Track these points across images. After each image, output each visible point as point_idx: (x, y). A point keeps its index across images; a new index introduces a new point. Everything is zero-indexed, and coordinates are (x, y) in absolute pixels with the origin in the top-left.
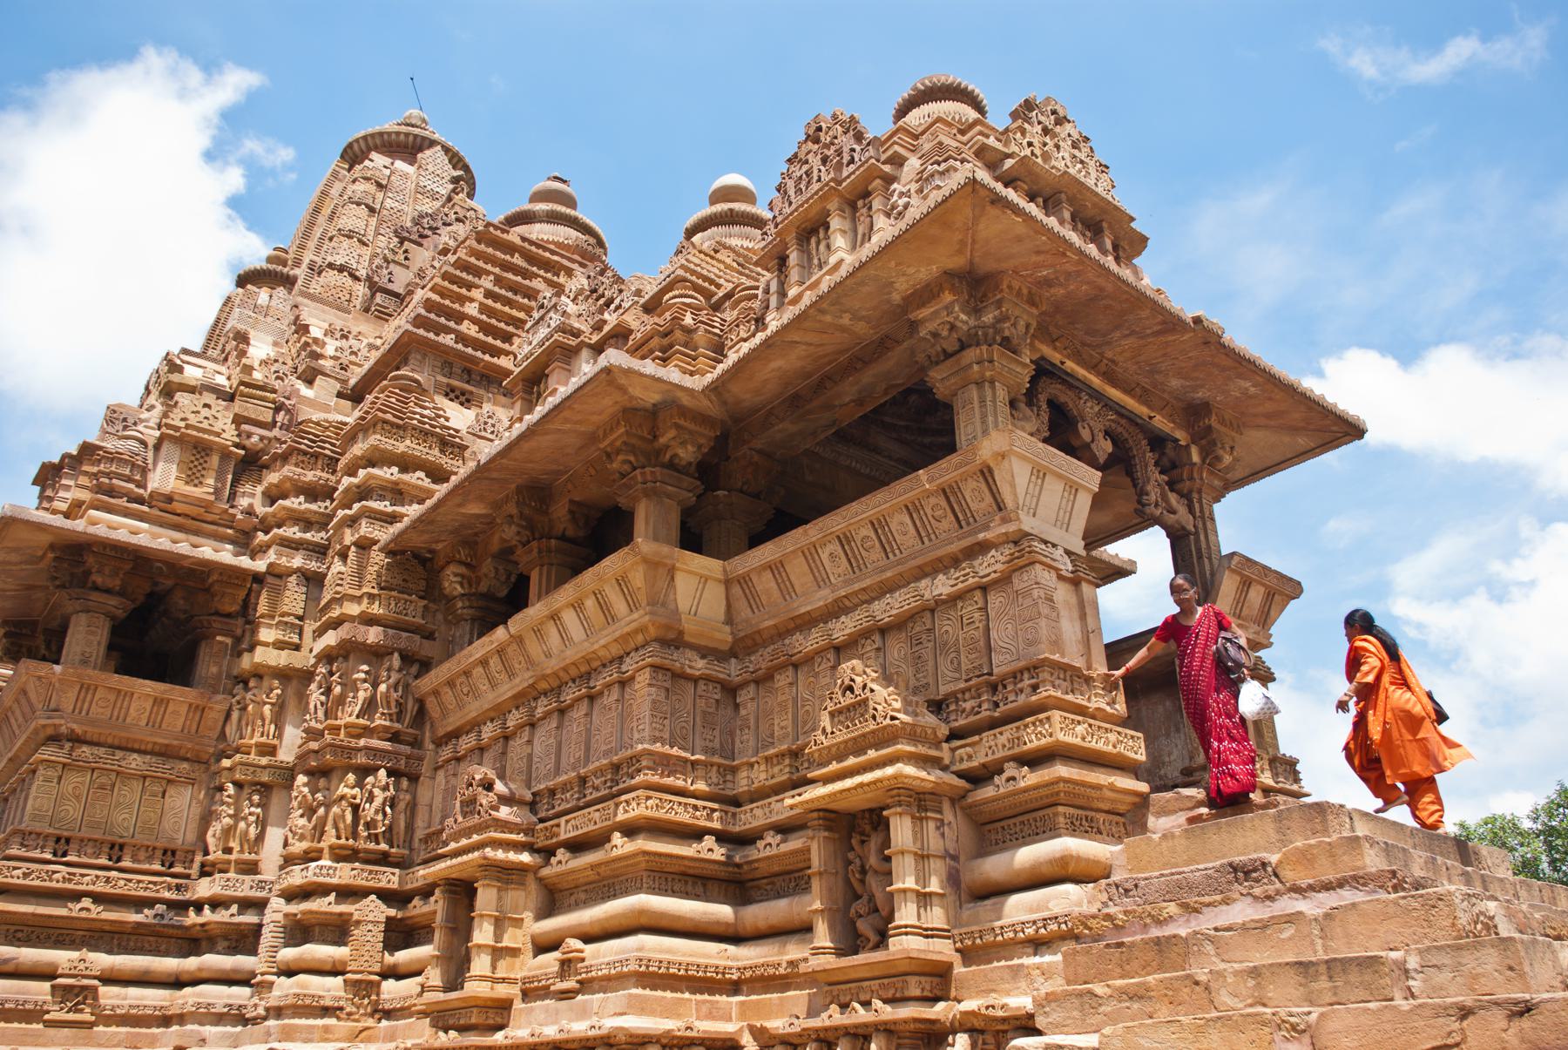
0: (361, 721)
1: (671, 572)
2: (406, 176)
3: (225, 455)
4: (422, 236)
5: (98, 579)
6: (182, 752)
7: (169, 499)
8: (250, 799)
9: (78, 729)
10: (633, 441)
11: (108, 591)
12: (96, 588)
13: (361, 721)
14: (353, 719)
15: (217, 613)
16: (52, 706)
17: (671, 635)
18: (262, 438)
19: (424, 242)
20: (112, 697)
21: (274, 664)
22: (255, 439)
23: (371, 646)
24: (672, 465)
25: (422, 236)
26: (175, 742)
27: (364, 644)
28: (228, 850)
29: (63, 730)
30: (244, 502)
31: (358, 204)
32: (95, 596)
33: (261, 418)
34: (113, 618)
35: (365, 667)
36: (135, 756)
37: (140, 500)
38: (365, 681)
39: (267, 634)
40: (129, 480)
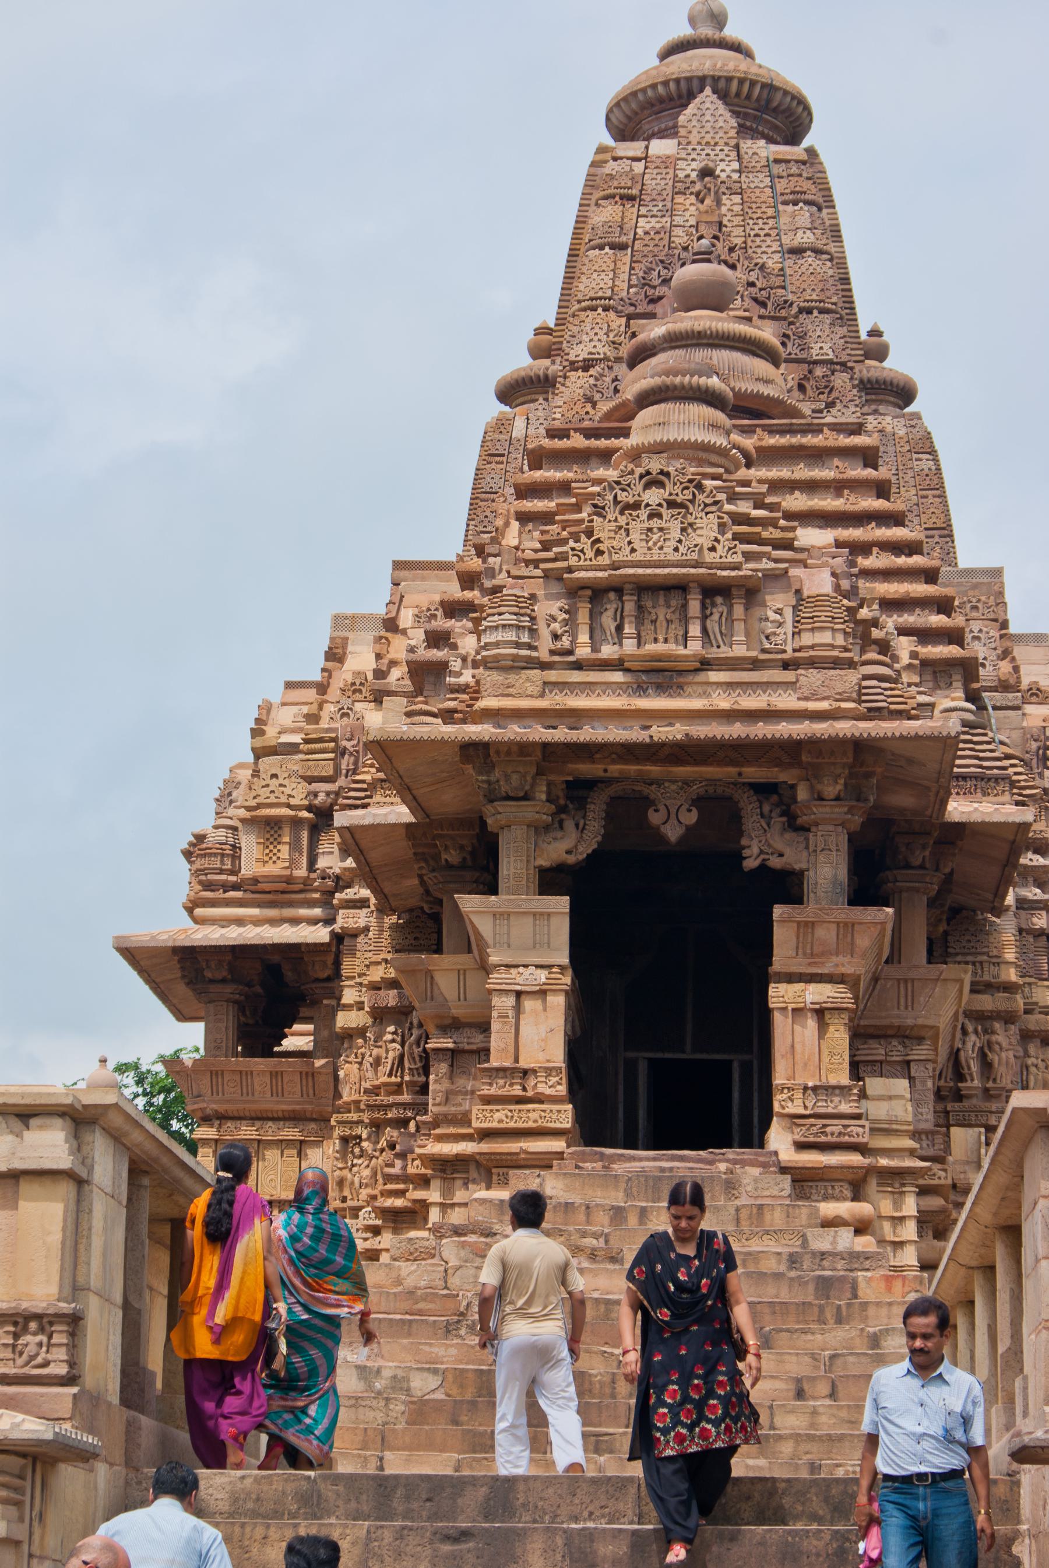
0: (393, 1079)
1: (429, 974)
2: (667, 162)
3: (296, 823)
4: (653, 301)
5: (208, 974)
6: (308, 1115)
7: (255, 880)
8: (352, 1152)
9: (221, 1108)
10: (420, 850)
11: (224, 981)
12: (212, 981)
13: (393, 1079)
14: (385, 1079)
15: (317, 980)
16: (195, 1093)
17: (448, 1021)
18: (328, 794)
19: (658, 308)
20: (237, 1078)
21: (354, 1025)
22: (321, 797)
23: (392, 1008)
24: (449, 866)
25: (653, 301)
26: (298, 1107)
27: (386, 1007)
28: (344, 1200)
29: (208, 1111)
30: (322, 863)
31: (601, 248)
32: (213, 988)
33: (324, 774)
34: (235, 1002)
35: (391, 1029)
36: (270, 1123)
37: (236, 887)
38: (393, 1041)
39: (349, 996)
40: (221, 871)
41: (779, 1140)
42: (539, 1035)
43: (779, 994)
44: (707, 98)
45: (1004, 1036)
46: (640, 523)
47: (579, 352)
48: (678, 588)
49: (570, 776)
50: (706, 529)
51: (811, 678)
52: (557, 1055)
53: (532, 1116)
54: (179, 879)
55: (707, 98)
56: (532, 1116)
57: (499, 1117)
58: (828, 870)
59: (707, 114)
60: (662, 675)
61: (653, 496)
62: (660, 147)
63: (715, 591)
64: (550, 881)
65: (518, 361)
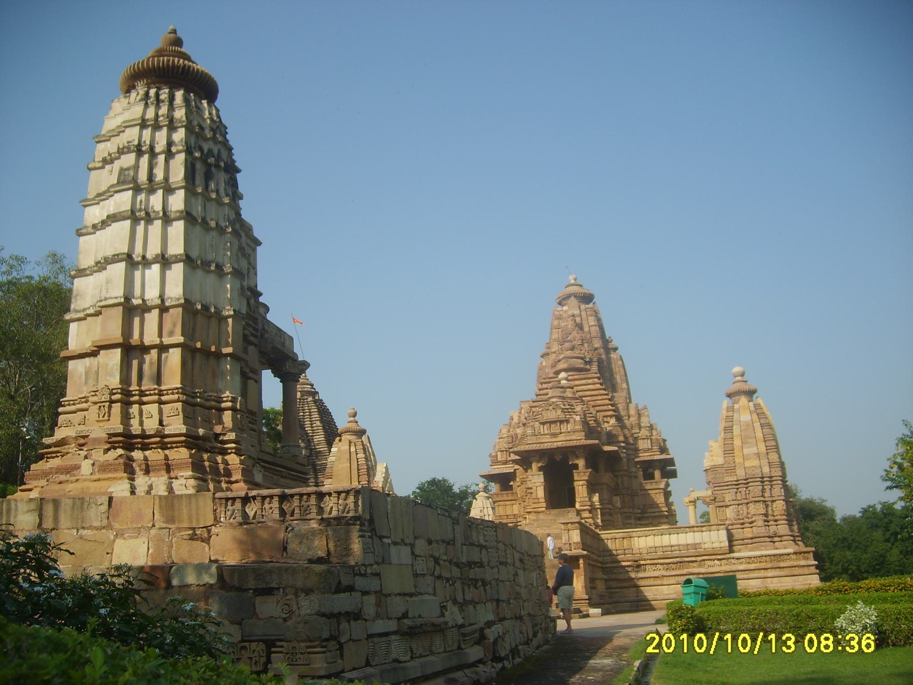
2: (566, 311)
41: (577, 506)
42: (541, 493)
43: (576, 483)
44: (573, 298)
45: (625, 478)
46: (548, 412)
47: (553, 350)
48: (555, 422)
49: (541, 454)
50: (559, 412)
51: (577, 434)
52: (543, 495)
53: (540, 505)
54: (488, 461)
55: (573, 298)
56: (540, 505)
57: (535, 506)
58: (581, 463)
59: (573, 301)
60: (554, 435)
61: (551, 408)
62: (565, 308)
63: (561, 422)
64: (540, 469)
65: (545, 350)
